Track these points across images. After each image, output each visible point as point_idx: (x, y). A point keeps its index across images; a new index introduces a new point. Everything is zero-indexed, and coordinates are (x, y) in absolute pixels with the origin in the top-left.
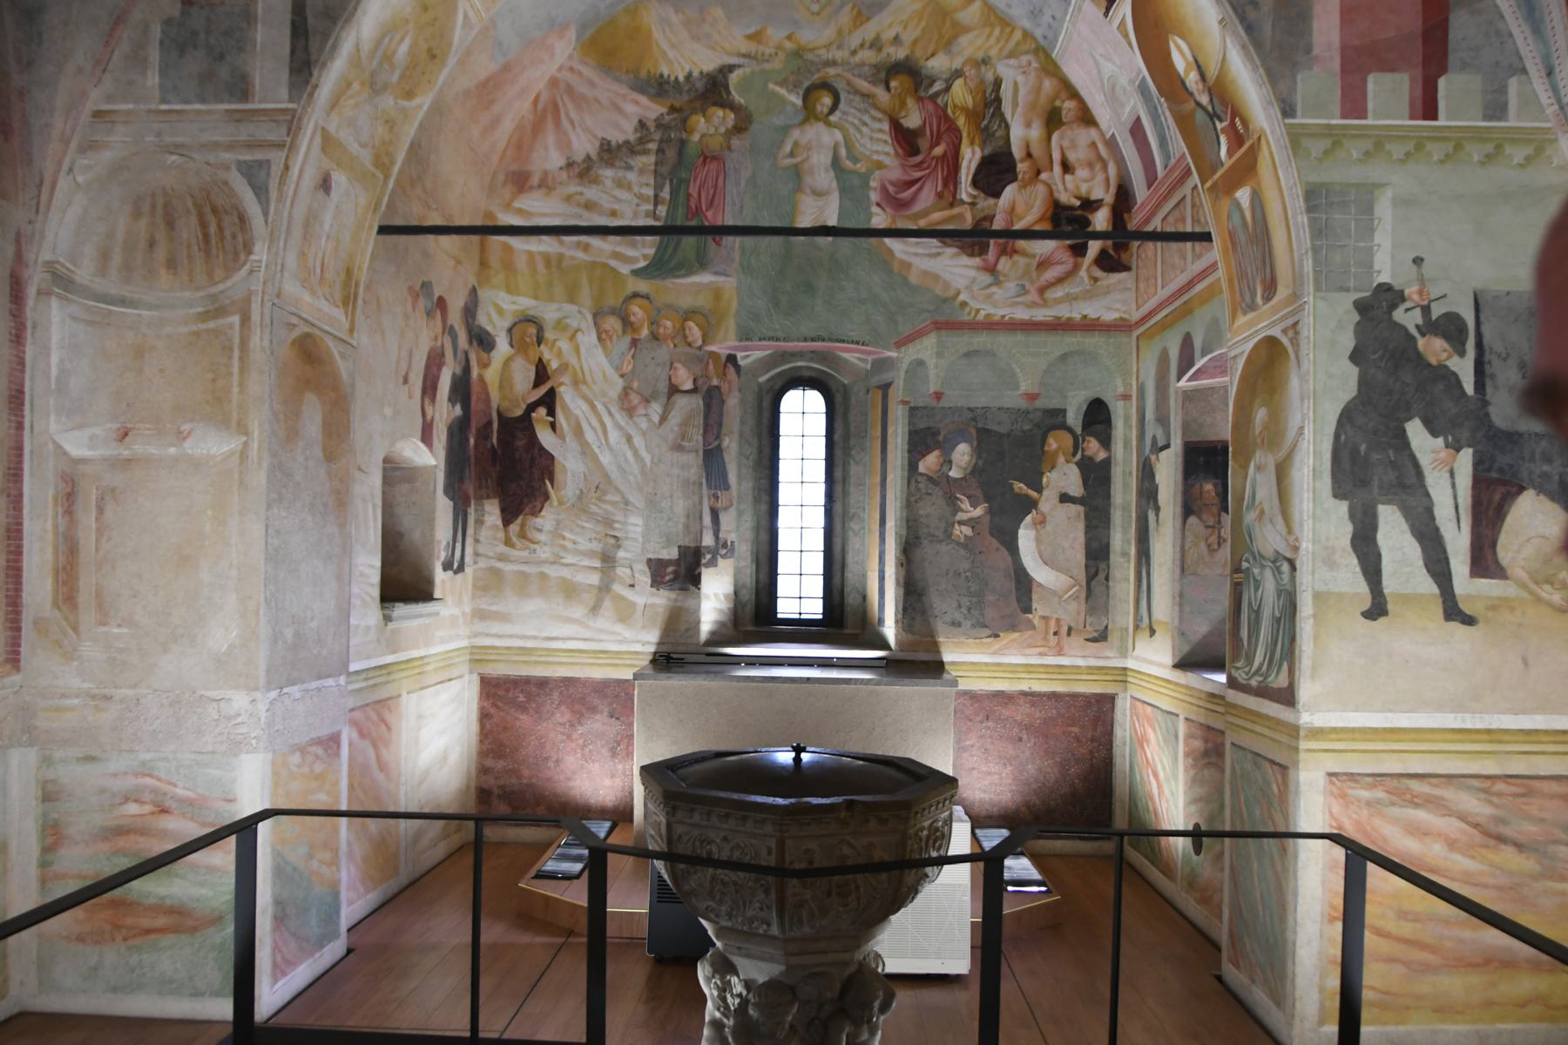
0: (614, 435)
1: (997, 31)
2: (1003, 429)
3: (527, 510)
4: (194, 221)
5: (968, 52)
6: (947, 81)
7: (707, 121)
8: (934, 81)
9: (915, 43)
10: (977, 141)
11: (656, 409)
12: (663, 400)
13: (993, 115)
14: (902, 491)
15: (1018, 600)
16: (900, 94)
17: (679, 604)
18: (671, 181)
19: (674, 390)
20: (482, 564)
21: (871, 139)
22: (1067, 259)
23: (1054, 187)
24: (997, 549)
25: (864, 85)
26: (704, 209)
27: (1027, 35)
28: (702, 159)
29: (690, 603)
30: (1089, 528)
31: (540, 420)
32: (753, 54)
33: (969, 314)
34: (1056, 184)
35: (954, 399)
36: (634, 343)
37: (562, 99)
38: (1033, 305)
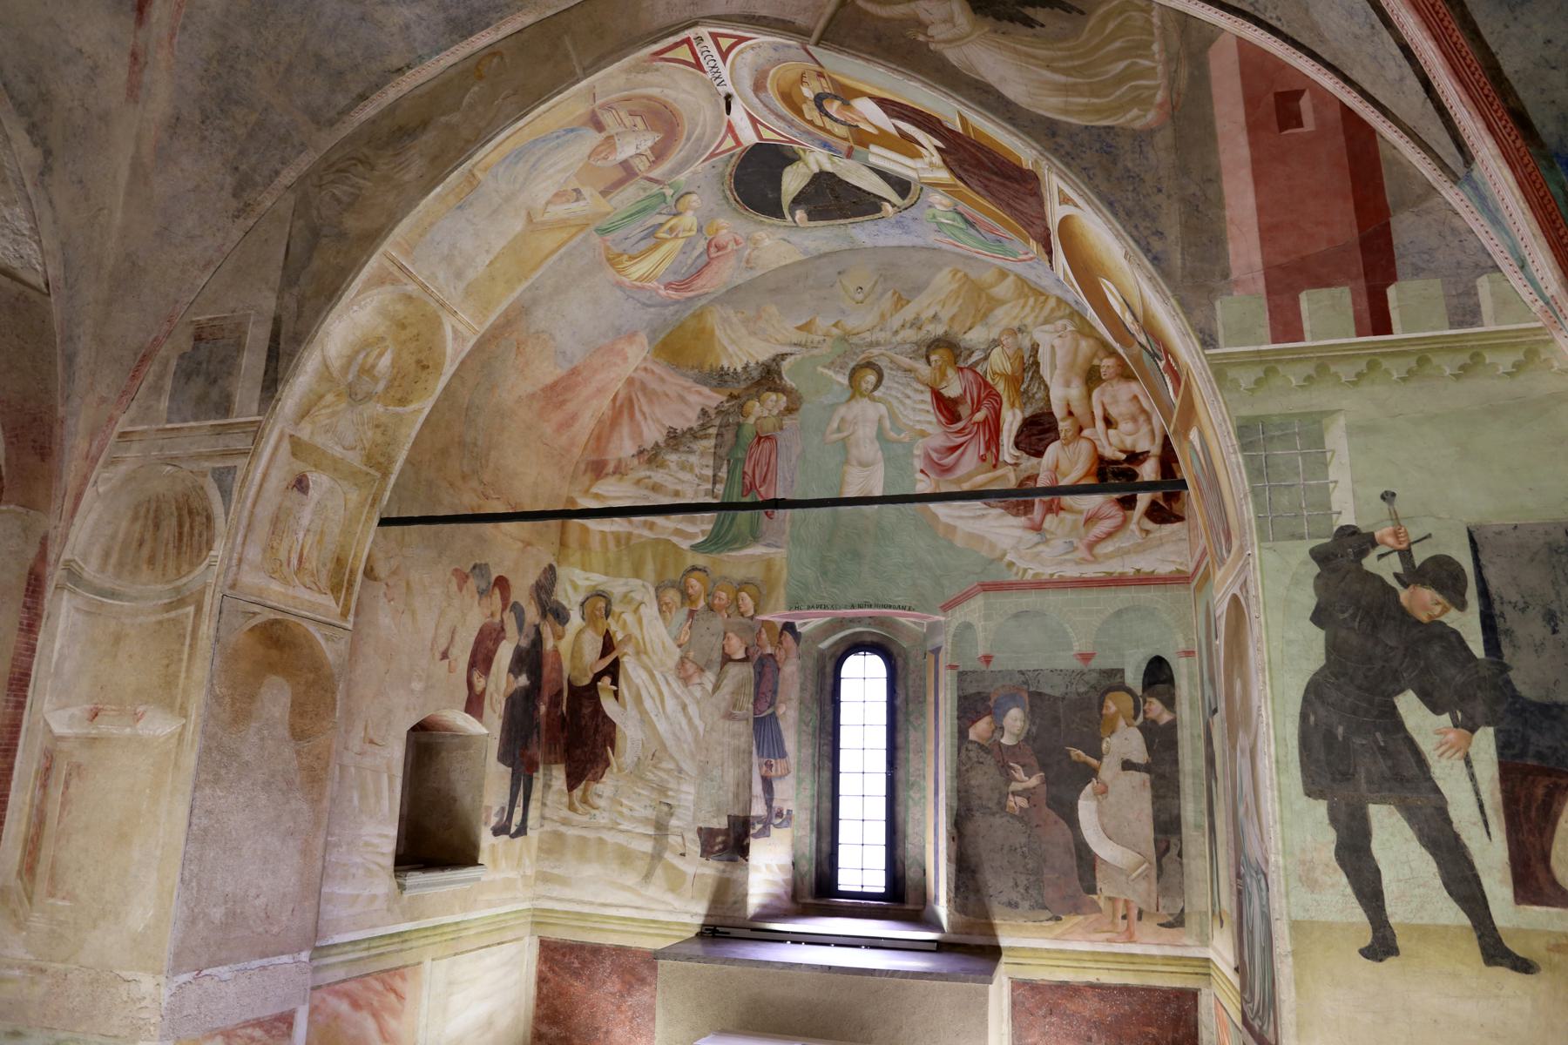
0: (670, 703)
1: (1031, 301)
2: (1057, 693)
3: (590, 776)
4: (174, 522)
5: (1004, 323)
7: (762, 405)
9: (953, 319)
10: (1017, 405)
11: (709, 678)
12: (717, 668)
14: (952, 761)
15: (1081, 879)
17: (726, 875)
19: (727, 659)
20: (548, 827)
21: (914, 409)
22: (1116, 511)
23: (1097, 443)
24: (1056, 822)
25: (905, 361)
27: (1060, 301)
29: (737, 874)
30: (1156, 798)
31: (605, 689)
33: (1017, 574)
35: (1002, 662)
36: (692, 614)
38: (1084, 561)
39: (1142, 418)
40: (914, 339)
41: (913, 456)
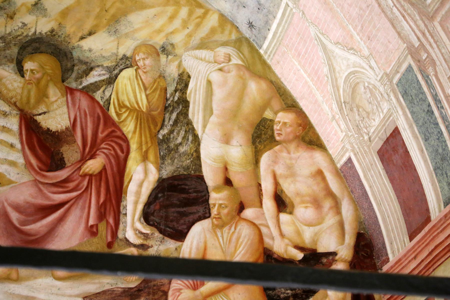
1: (184, 12)
6: (109, 70)
8: (92, 69)
9: (65, 13)
10: (151, 156)
13: (176, 122)
16: (39, 81)
23: (264, 230)
34: (268, 227)
39: (327, 204)
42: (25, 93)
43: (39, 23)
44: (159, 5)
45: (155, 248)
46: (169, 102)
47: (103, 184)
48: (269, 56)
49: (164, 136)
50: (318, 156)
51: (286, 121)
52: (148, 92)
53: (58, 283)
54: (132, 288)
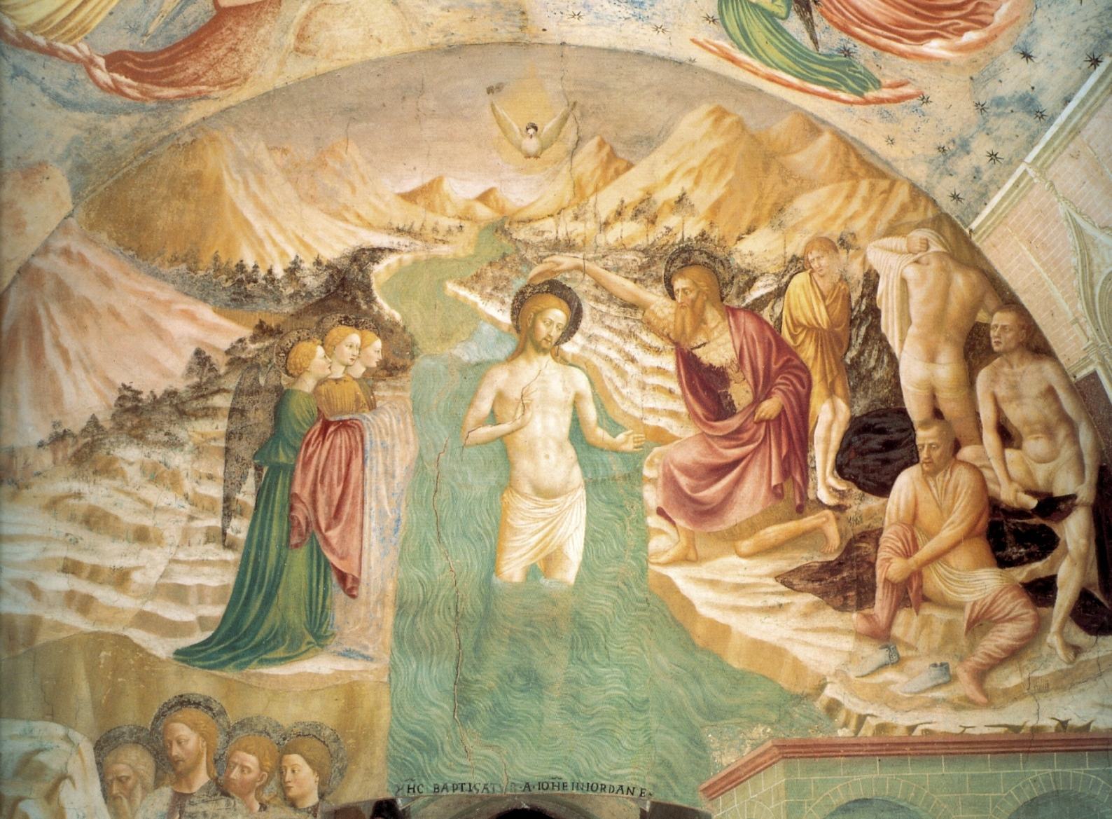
7: (329, 354)
8: (755, 279)
9: (716, 208)
10: (839, 390)
13: (866, 339)
16: (693, 302)
18: (258, 468)
21: (643, 386)
23: (987, 473)
25: (625, 286)
26: (323, 525)
28: (318, 426)
32: (417, 227)
34: (991, 468)
36: (180, 800)
37: (47, 309)
38: (965, 704)
40: (642, 242)
41: (642, 480)
42: (679, 319)
43: (686, 225)
44: (832, 182)
45: (854, 508)
46: (855, 313)
47: (783, 432)
48: (980, 237)
49: (852, 360)
50: (1048, 368)
51: (1006, 323)
52: (828, 302)
53: (744, 562)
54: (832, 562)
